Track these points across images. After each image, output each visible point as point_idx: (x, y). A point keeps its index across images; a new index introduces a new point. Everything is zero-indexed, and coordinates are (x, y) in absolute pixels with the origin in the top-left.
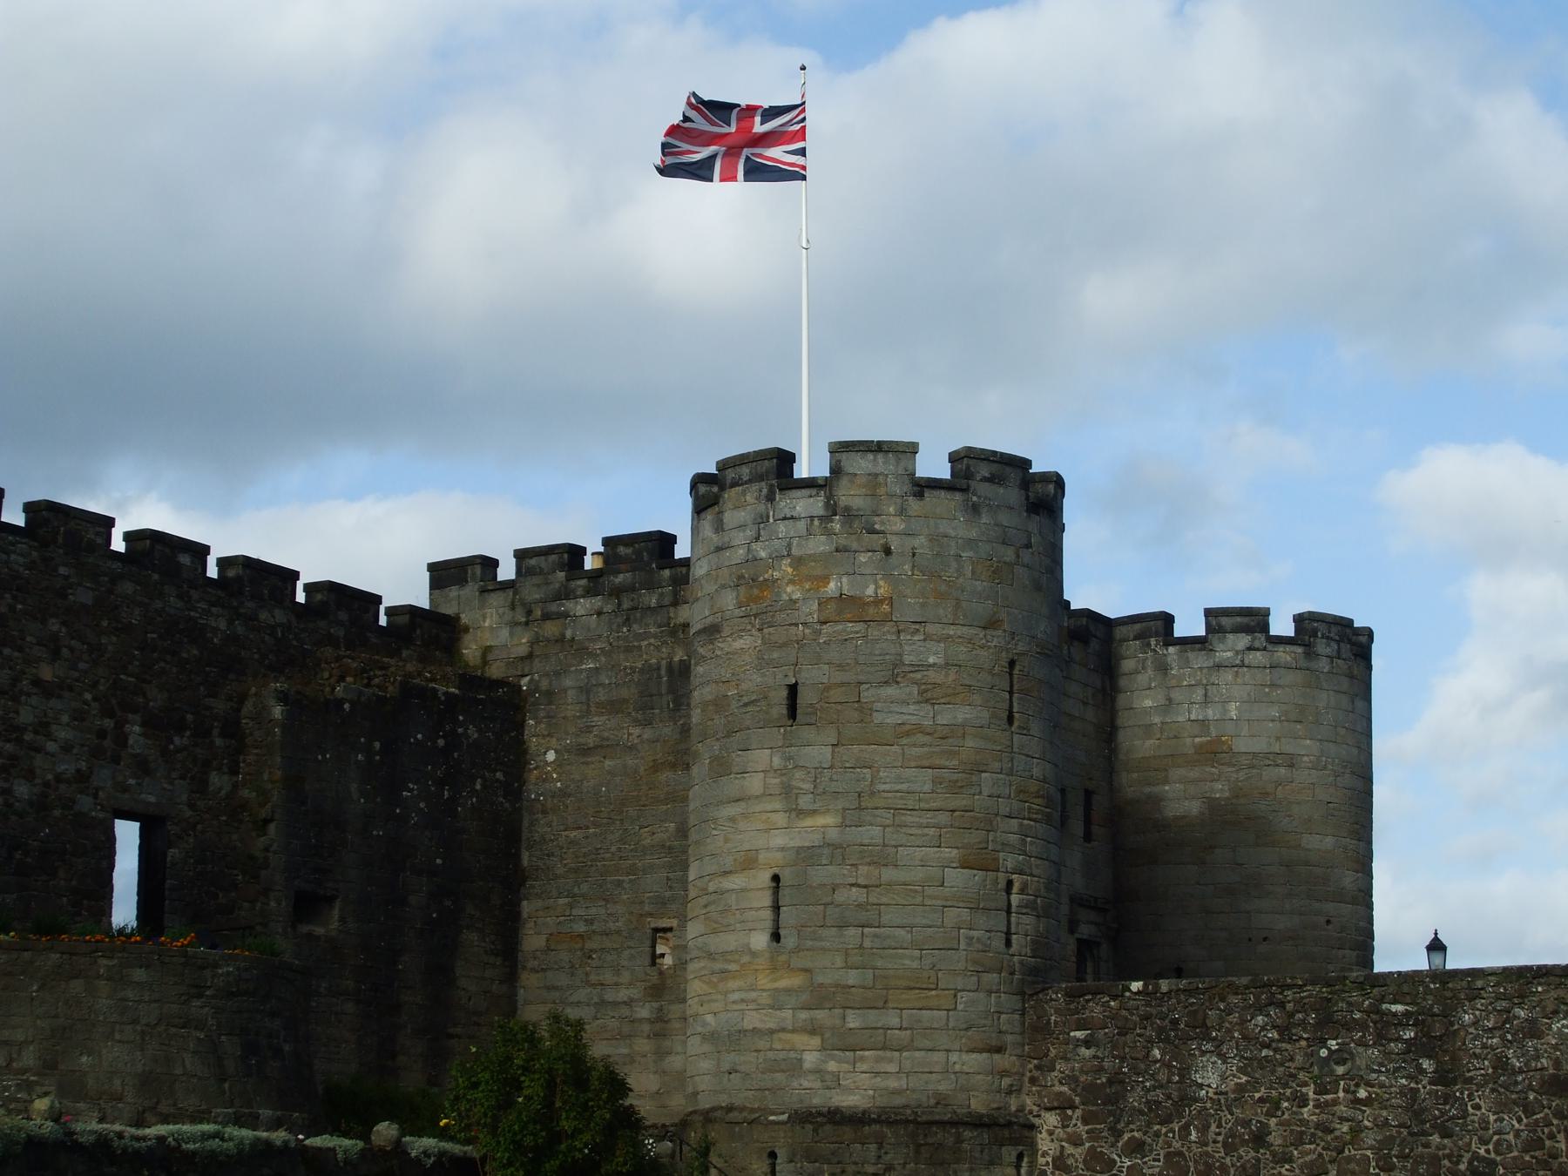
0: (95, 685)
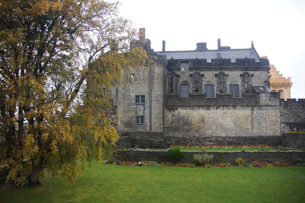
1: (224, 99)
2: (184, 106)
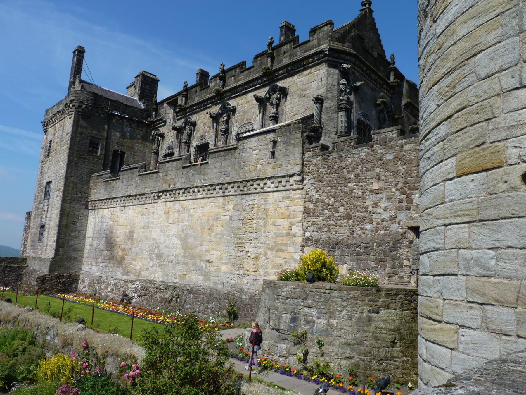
0: (397, 185)
1: (169, 173)
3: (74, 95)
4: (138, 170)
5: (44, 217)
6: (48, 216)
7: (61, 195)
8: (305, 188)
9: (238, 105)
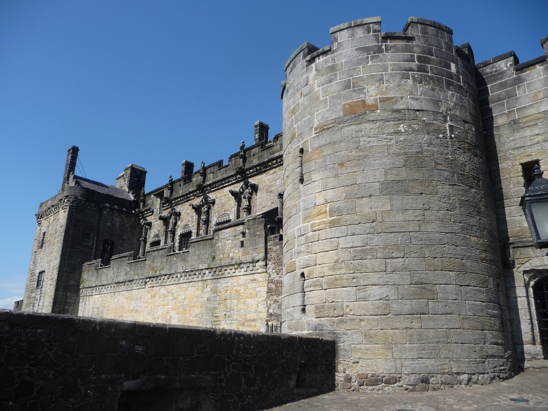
1: (156, 260)
2: (100, 286)
3: (70, 191)
4: (127, 258)
5: (36, 305)
6: (41, 304)
7: (54, 284)
8: (268, 271)
9: (217, 198)
